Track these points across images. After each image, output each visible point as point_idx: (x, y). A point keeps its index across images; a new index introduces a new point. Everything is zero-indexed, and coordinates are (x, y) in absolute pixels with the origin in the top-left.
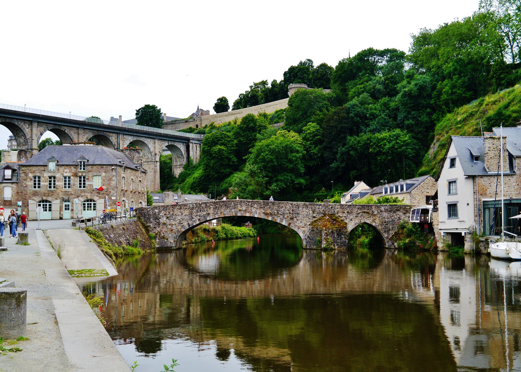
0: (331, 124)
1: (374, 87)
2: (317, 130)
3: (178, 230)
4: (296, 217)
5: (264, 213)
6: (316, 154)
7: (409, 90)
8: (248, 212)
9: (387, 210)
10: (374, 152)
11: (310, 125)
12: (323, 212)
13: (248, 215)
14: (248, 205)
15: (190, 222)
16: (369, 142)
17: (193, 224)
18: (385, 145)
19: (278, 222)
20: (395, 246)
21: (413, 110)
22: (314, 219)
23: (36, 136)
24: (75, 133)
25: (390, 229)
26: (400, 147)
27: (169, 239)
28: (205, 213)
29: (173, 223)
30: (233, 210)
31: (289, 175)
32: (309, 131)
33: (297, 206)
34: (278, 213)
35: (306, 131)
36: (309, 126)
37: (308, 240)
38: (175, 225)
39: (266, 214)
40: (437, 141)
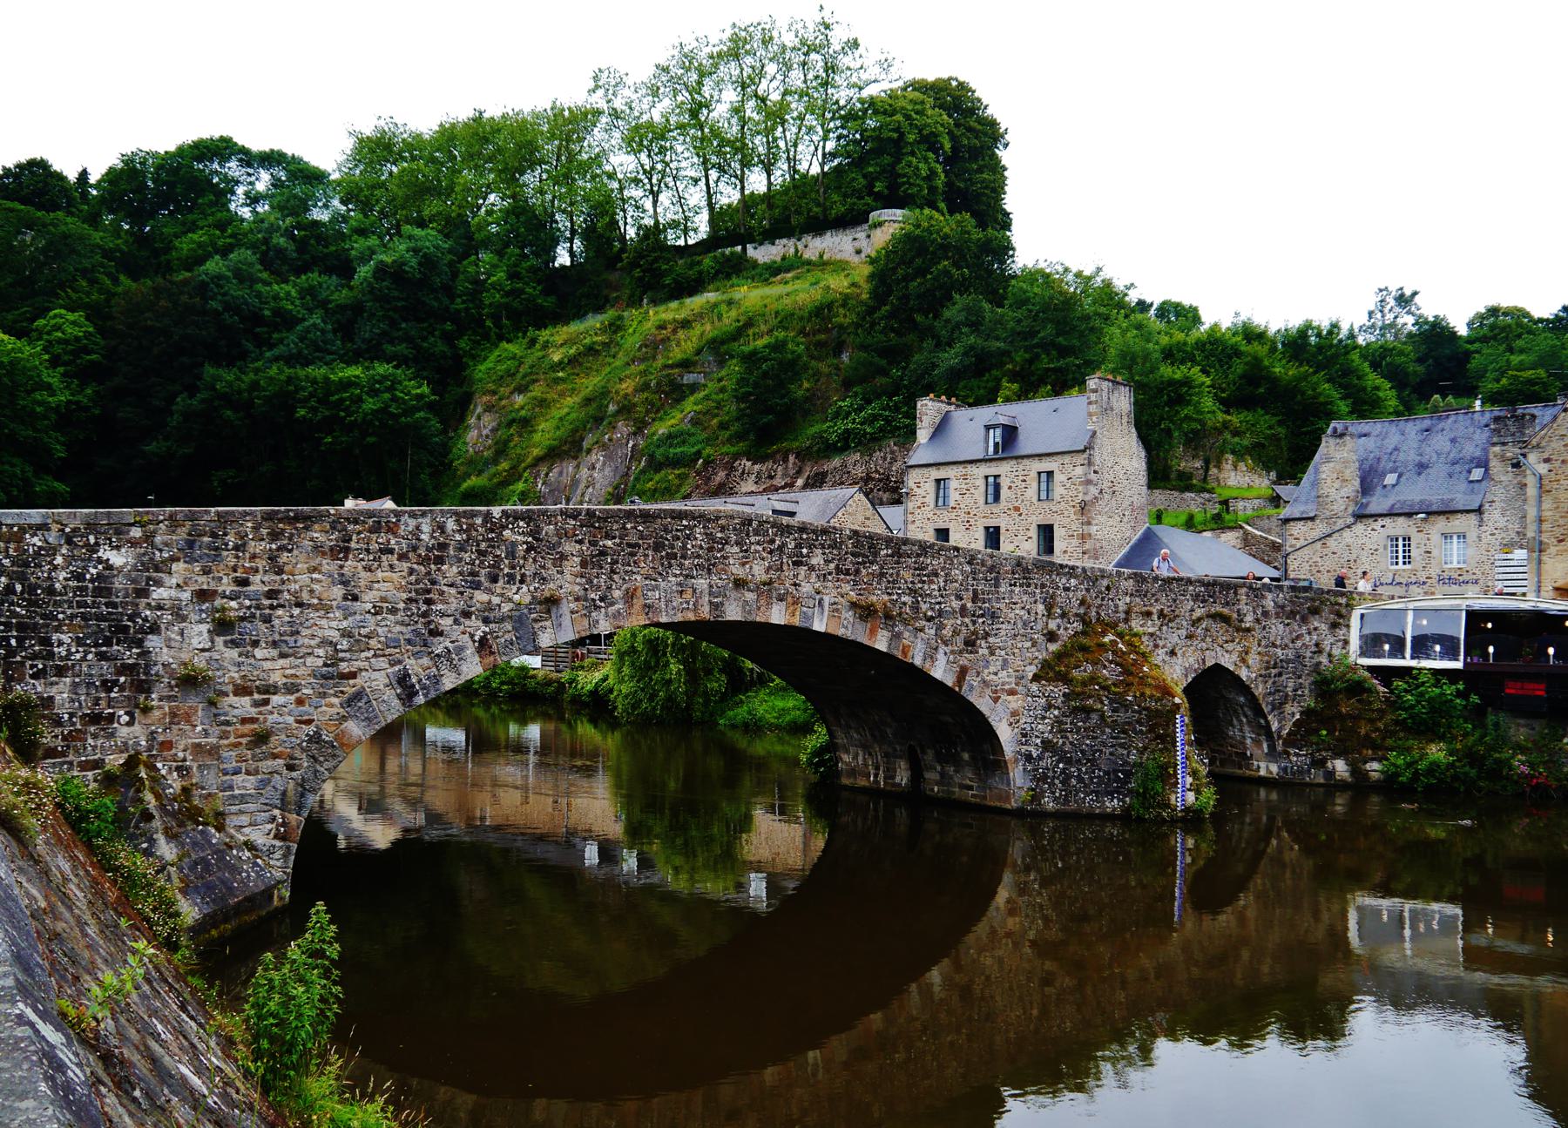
0: (149, 322)
1: (266, 241)
2: (88, 335)
3: (315, 738)
4: (987, 635)
5: (854, 605)
6: (87, 409)
7: (394, 261)
8: (781, 599)
9: (1282, 607)
10: (311, 420)
11: (61, 316)
12: (1082, 611)
13: (777, 615)
14: (781, 548)
15: (417, 667)
16: (291, 388)
17: (436, 680)
18: (360, 400)
19: (918, 661)
20: (1331, 774)
21: (405, 320)
22: (1053, 647)
25: (1287, 695)
26: (406, 413)
27: (231, 822)
28: (522, 595)
29: (278, 671)
30: (702, 583)
31: (16, 460)
32: (60, 334)
33: (992, 569)
34: (915, 607)
35: (49, 333)
36: (58, 320)
37: (1047, 761)
38: (291, 689)
39: (866, 612)
40: (485, 411)
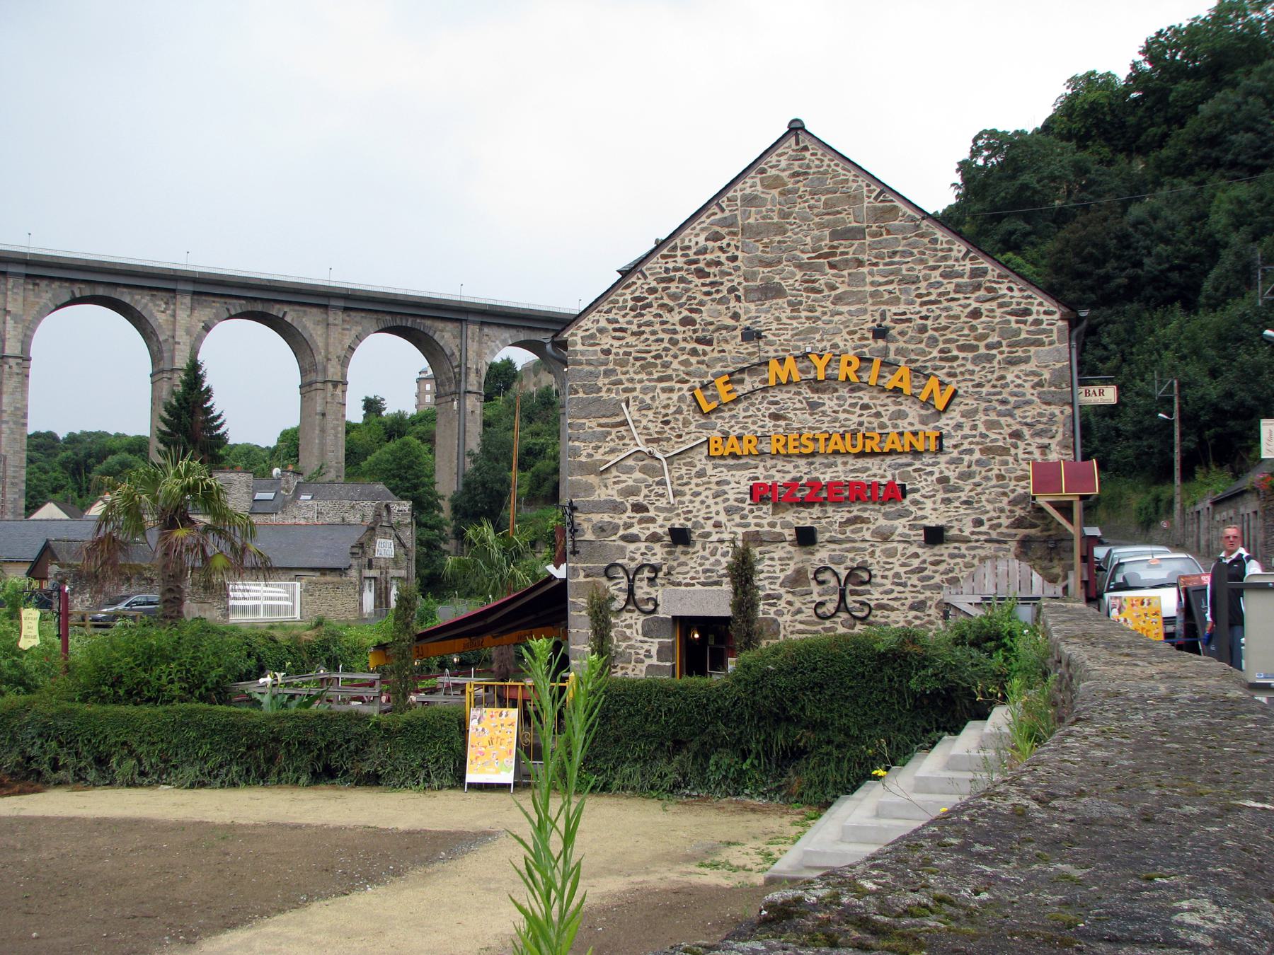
23: (188, 332)
24: (318, 323)
